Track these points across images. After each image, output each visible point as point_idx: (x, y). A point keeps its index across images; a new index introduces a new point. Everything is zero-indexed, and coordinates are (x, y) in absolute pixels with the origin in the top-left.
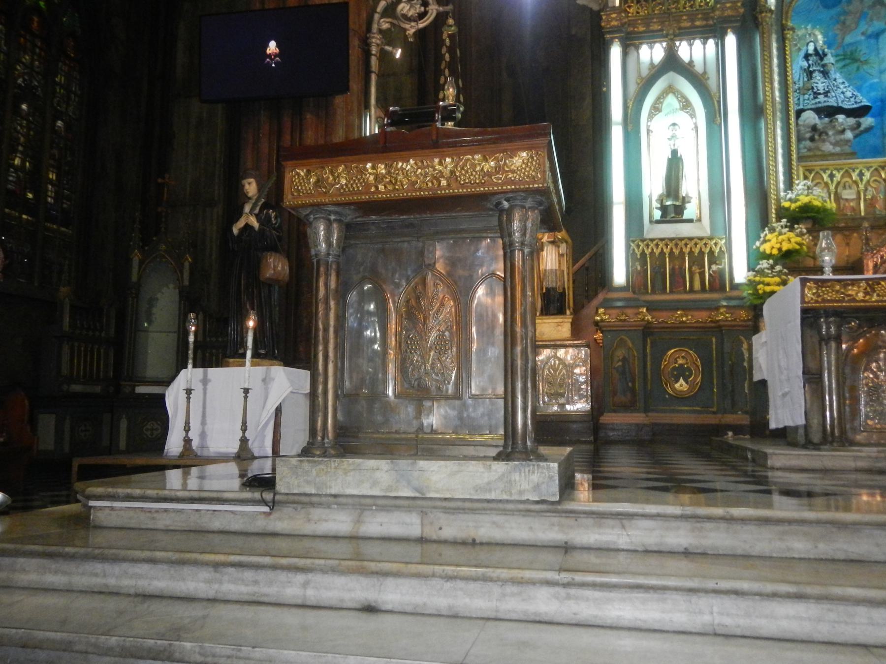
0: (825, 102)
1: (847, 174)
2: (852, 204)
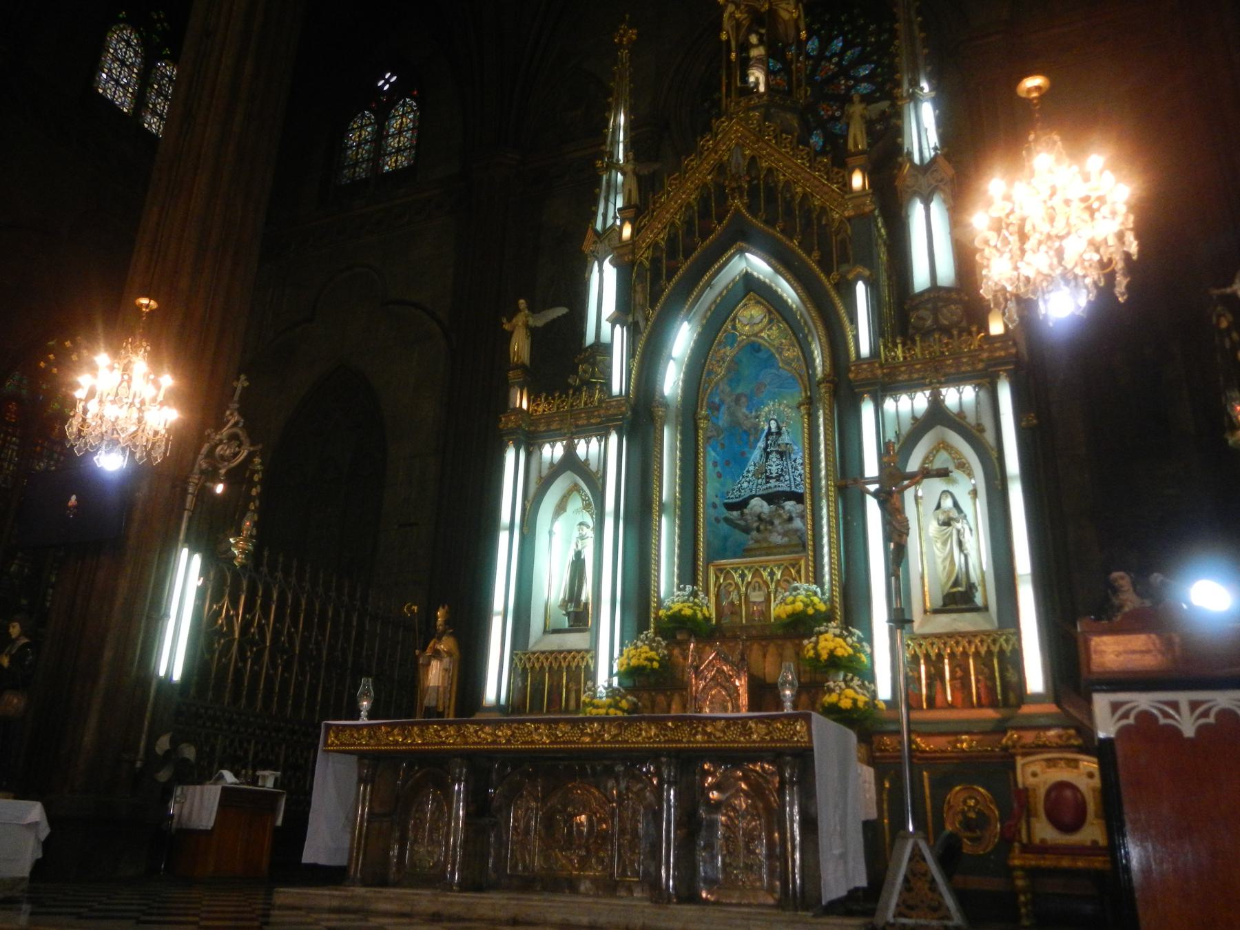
0: (775, 486)
1: (756, 573)
2: (759, 608)
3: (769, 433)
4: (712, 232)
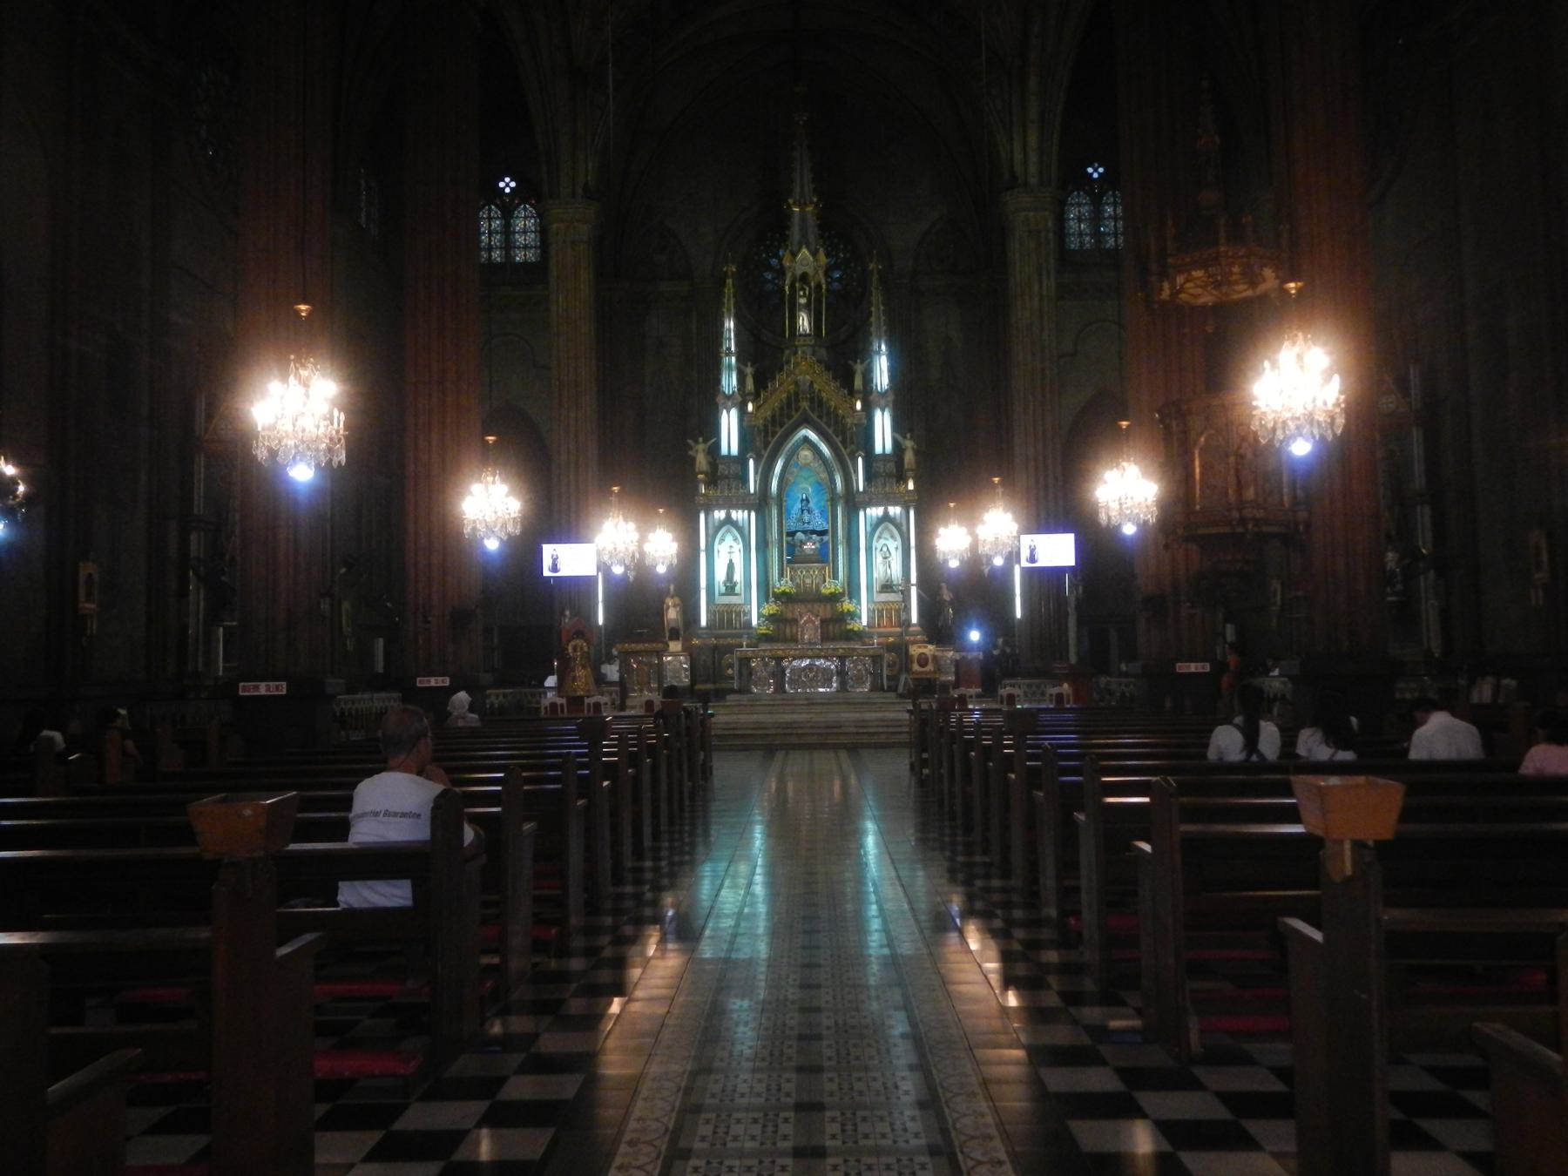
3: (802, 500)
4: (792, 417)
